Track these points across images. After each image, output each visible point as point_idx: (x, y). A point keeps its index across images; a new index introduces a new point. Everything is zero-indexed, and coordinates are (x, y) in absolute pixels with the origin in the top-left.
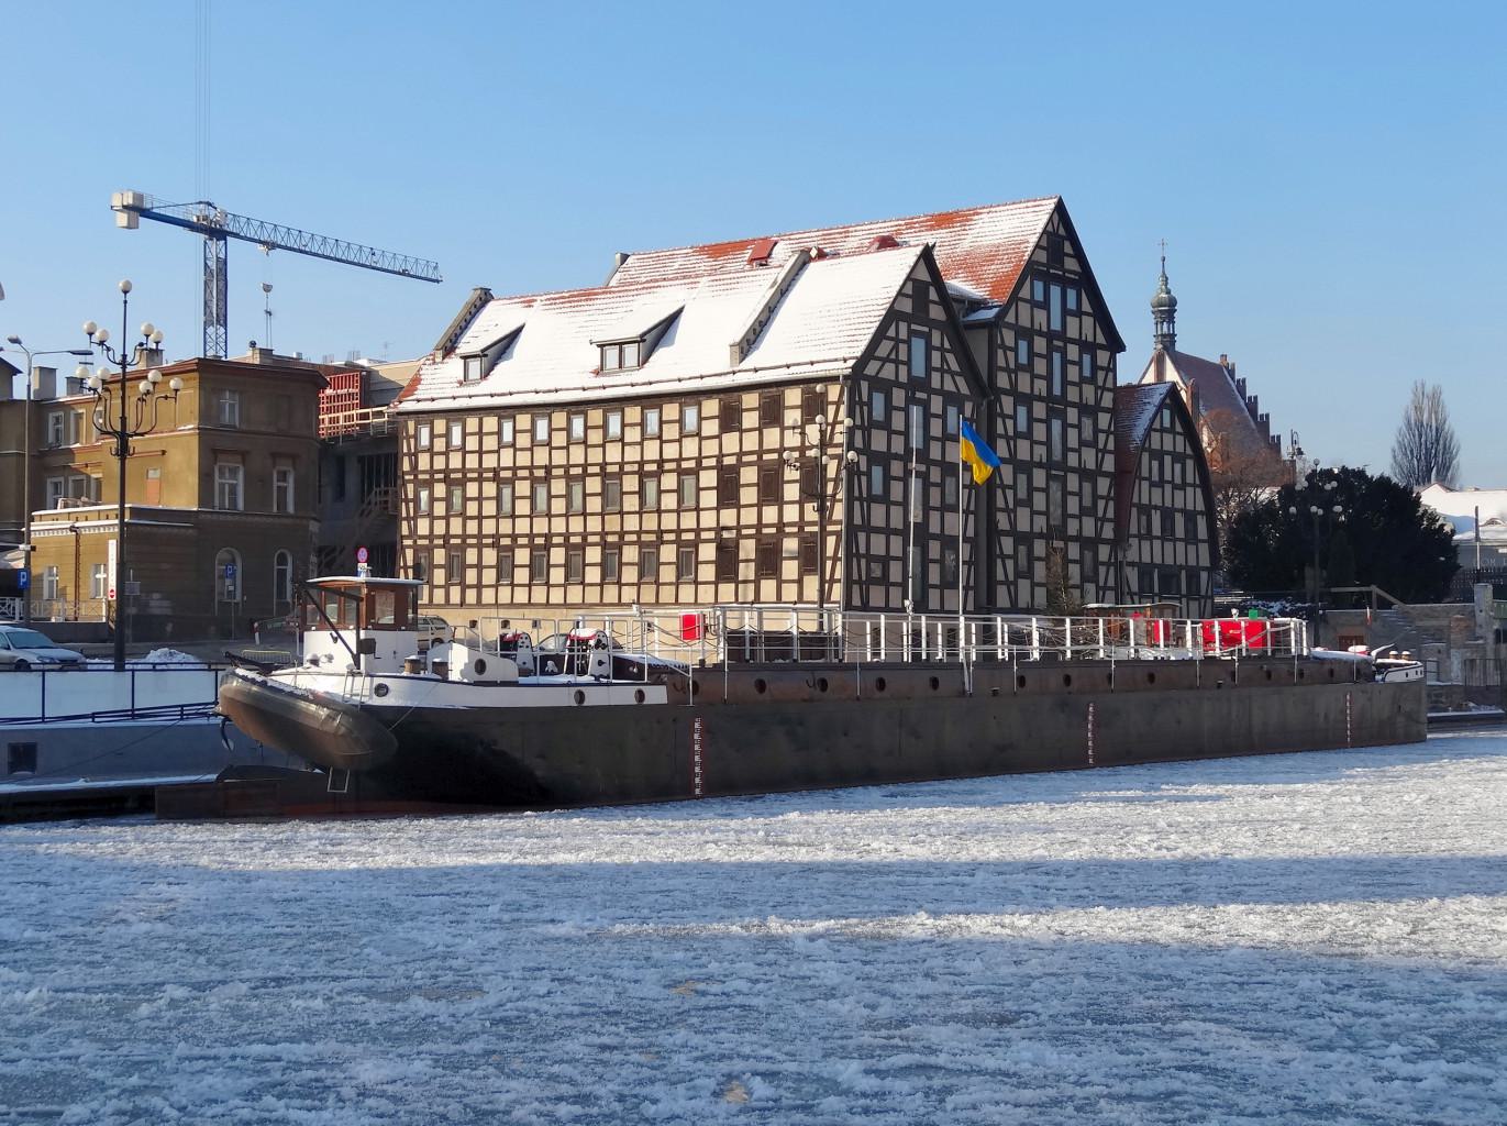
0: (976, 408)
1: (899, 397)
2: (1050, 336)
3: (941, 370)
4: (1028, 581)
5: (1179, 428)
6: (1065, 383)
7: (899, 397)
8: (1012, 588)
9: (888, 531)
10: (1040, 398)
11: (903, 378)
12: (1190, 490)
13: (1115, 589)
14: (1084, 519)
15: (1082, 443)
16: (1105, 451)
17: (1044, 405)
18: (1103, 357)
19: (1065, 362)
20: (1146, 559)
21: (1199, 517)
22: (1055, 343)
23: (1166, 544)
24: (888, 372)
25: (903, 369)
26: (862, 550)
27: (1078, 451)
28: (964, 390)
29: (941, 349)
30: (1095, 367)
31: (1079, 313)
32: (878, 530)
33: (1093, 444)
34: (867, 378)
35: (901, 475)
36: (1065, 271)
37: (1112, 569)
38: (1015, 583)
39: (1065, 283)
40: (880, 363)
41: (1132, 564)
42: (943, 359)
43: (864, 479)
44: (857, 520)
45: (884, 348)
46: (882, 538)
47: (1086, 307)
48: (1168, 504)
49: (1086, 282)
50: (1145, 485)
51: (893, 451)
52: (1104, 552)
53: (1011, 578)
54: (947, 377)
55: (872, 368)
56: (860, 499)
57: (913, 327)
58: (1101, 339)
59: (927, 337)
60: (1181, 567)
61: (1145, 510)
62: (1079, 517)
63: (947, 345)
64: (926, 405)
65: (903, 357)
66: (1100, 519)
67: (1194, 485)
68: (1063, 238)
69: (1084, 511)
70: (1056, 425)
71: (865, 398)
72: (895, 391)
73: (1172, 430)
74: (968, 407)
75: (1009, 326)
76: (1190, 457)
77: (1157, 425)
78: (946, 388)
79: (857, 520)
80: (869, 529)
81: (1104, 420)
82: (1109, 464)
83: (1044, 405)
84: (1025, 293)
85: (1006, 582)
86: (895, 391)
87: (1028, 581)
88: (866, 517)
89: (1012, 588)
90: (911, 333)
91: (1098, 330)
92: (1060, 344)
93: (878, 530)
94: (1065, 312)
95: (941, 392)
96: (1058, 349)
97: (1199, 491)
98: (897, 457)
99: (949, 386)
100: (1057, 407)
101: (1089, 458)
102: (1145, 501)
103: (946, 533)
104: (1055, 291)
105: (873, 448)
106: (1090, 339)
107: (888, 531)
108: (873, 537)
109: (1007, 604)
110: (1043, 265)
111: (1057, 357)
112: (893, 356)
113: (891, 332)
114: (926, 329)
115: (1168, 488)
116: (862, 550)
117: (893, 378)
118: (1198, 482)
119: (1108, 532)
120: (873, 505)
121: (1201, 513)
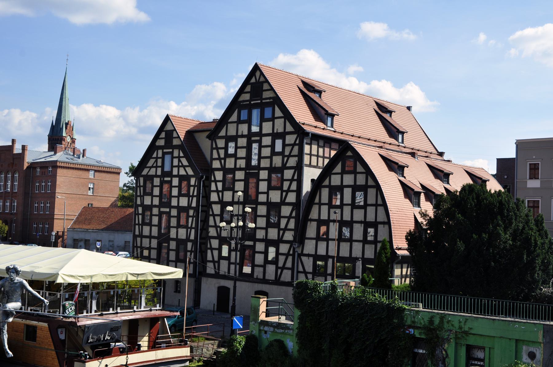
0: (199, 179)
1: (157, 181)
2: (250, 135)
3: (178, 167)
4: (227, 262)
5: (360, 168)
6: (260, 158)
7: (157, 181)
8: (216, 264)
9: (150, 237)
10: (240, 169)
11: (159, 172)
12: (371, 210)
13: (292, 269)
14: (270, 230)
15: (270, 188)
16: (289, 191)
17: (244, 172)
18: (290, 139)
19: (260, 147)
20: (322, 251)
21: (380, 227)
22: (253, 139)
23: (342, 244)
24: (152, 172)
25: (159, 170)
26: (139, 245)
27: (267, 193)
28: (190, 172)
29: (179, 157)
30: (284, 145)
31: (273, 119)
32: (146, 237)
33: (280, 188)
34: (143, 176)
35: (157, 213)
36: (262, 99)
37: (290, 258)
38: (219, 262)
39: (262, 107)
40: (148, 169)
41: (308, 255)
42: (180, 161)
43: (140, 217)
44: (137, 233)
45: (151, 162)
46: (148, 240)
47: (278, 113)
48: (347, 217)
49: (277, 101)
50: (325, 209)
51: (154, 204)
52: (284, 248)
53: (216, 259)
54: (182, 169)
55: (145, 172)
56: (139, 224)
57: (165, 151)
58: (289, 128)
59: (172, 153)
60: (357, 259)
61: (320, 222)
62: (266, 229)
63: (182, 155)
64: (171, 182)
65: (159, 164)
66: (282, 229)
67: (376, 205)
68: (263, 82)
69: (269, 225)
70: (252, 181)
71: (142, 184)
72: (155, 179)
73: (354, 172)
74: (193, 181)
75: (222, 137)
76: (371, 187)
77: (338, 169)
78: (180, 174)
79: (137, 233)
80: (142, 236)
81: (288, 174)
82: (291, 198)
83: (244, 172)
84: (234, 118)
85: (213, 261)
86: (155, 179)
87: (227, 262)
88: (141, 232)
89: (216, 264)
90: (164, 154)
91: (288, 124)
92: (258, 138)
93: (146, 237)
94: (263, 119)
95: (178, 176)
96: (255, 142)
97: (381, 210)
98: (155, 206)
99: (182, 172)
100: (252, 173)
101: (275, 196)
102: (324, 216)
103: (179, 237)
104: (256, 113)
105: (145, 204)
106: (281, 130)
107: (150, 237)
108: (144, 239)
109: (213, 272)
110: (247, 101)
111: (255, 146)
112: (155, 165)
113: (155, 155)
114: (171, 150)
115: (347, 210)
116: (139, 245)
117: (154, 174)
118: (380, 202)
119: (289, 236)
120: (144, 227)
121: (383, 223)
